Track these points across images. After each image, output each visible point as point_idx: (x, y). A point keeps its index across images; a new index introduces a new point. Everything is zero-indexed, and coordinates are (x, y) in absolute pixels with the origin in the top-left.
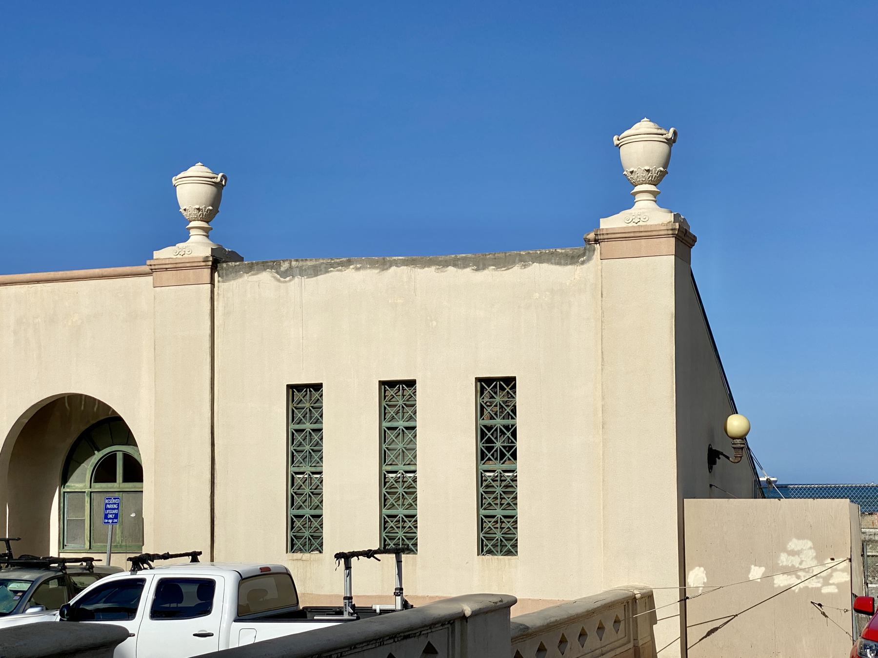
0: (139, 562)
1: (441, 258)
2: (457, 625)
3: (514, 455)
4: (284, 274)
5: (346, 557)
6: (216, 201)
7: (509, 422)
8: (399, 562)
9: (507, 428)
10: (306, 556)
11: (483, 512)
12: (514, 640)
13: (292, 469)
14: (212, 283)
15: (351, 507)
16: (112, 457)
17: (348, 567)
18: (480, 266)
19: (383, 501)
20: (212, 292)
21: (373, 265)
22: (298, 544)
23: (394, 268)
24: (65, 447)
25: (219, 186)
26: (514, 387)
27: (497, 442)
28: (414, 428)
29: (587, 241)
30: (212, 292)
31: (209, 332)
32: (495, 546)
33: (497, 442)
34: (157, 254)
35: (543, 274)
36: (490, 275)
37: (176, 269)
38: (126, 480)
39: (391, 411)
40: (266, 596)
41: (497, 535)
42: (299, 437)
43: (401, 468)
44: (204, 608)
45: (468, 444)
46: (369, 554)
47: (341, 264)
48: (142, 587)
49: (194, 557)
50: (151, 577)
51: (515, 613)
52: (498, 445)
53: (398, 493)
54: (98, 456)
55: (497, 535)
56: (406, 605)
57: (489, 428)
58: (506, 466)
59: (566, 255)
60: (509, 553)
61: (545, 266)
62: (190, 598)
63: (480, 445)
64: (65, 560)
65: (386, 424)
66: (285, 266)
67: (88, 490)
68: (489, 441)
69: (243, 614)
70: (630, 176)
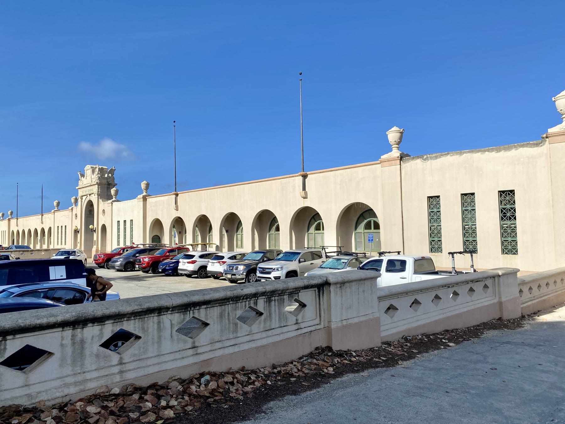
0: (381, 254)
2: (496, 279)
3: (515, 218)
4: (425, 160)
5: (452, 254)
6: (401, 138)
7: (513, 206)
8: (472, 256)
9: (512, 208)
10: (436, 254)
11: (503, 239)
12: (519, 284)
14: (400, 164)
15: (452, 237)
16: (370, 222)
17: (453, 257)
18: (498, 151)
19: (464, 235)
21: (457, 154)
22: (433, 250)
23: (465, 154)
24: (355, 219)
25: (401, 133)
26: (514, 194)
27: (508, 213)
28: (474, 210)
29: (543, 138)
32: (508, 251)
33: (508, 213)
34: (382, 157)
36: (502, 154)
37: (389, 161)
38: (374, 229)
39: (466, 204)
40: (424, 266)
42: (432, 214)
43: (470, 224)
44: (403, 269)
45: (496, 214)
46: (460, 253)
47: (445, 154)
48: (382, 262)
49: (399, 253)
50: (385, 259)
51: (519, 275)
52: (508, 215)
54: (366, 221)
56: (475, 271)
57: (504, 209)
58: (512, 222)
59: (534, 144)
60: (514, 254)
61: (525, 148)
62: (398, 266)
63: (501, 215)
64: (357, 253)
65: (464, 209)
66: (425, 157)
68: (505, 213)
69: (416, 272)
70: (560, 112)
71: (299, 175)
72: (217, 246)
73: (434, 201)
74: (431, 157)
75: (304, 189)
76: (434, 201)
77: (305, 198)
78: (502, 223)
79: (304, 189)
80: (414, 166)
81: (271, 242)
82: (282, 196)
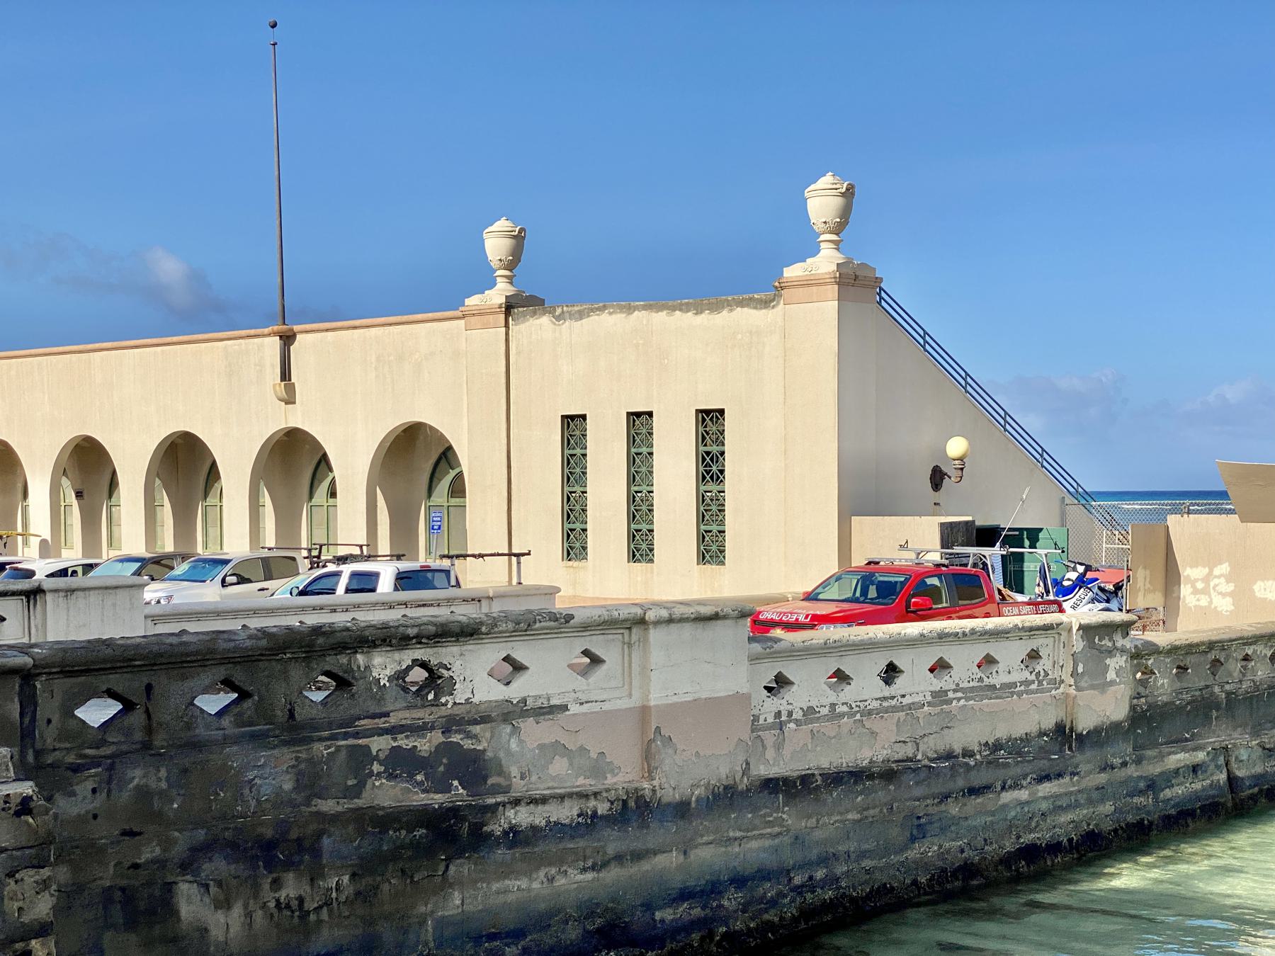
1: (670, 303)
4: (558, 318)
11: (703, 527)
13: (566, 489)
14: (507, 325)
18: (699, 312)
20: (507, 334)
21: (622, 309)
27: (710, 467)
30: (507, 334)
31: (504, 369)
33: (710, 467)
34: (468, 302)
35: (745, 317)
36: (705, 318)
37: (480, 314)
41: (711, 548)
47: (598, 309)
53: (639, 509)
55: (711, 548)
66: (559, 311)
67: (446, 504)
71: (275, 334)
72: (44, 542)
73: (573, 425)
74: (569, 312)
75: (285, 374)
76: (573, 425)
77: (290, 399)
78: (703, 488)
79: (285, 374)
80: (534, 330)
81: (210, 530)
82: (224, 394)
